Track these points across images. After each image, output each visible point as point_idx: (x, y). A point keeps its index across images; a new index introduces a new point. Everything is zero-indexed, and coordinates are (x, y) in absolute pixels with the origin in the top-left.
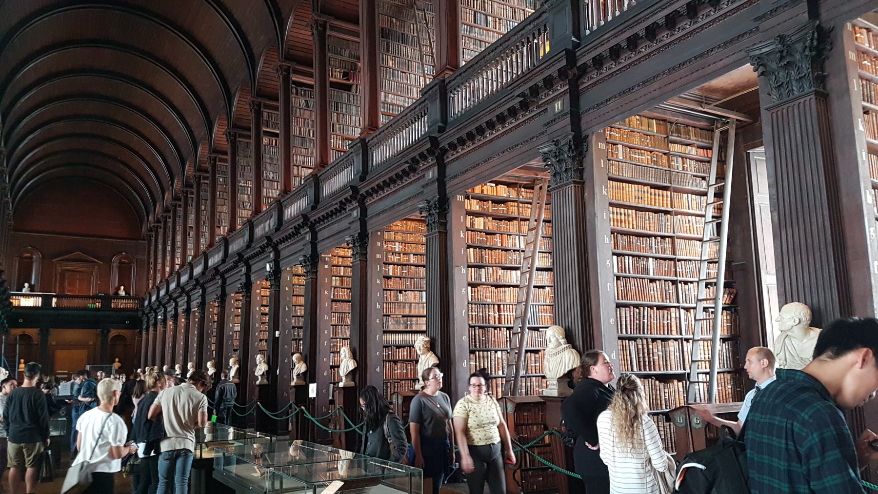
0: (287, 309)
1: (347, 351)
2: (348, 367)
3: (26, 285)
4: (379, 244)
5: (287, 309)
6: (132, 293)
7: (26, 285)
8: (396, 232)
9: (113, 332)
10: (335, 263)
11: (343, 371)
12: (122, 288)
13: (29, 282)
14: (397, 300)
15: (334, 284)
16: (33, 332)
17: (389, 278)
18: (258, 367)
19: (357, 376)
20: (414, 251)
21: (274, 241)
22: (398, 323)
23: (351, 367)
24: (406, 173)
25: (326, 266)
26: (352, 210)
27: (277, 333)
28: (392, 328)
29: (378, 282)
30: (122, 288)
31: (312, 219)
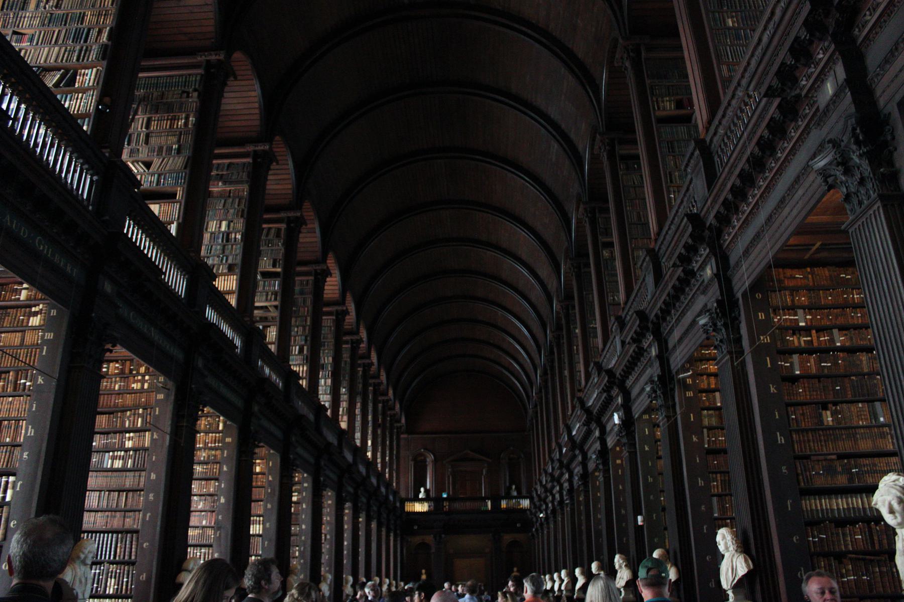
0: (650, 480)
1: (729, 537)
2: (734, 570)
3: (422, 490)
4: (761, 316)
5: (650, 480)
6: (524, 493)
7: (422, 490)
8: (794, 290)
9: (507, 538)
10: (704, 385)
11: (726, 581)
12: (514, 487)
14: (822, 422)
15: (706, 422)
16: (429, 539)
17: (794, 379)
18: (618, 575)
19: (758, 587)
20: (841, 321)
21: (618, 375)
22: (830, 471)
23: (742, 570)
24: (778, 129)
25: (690, 394)
26: (702, 267)
27: (640, 518)
28: (820, 482)
29: (772, 390)
30: (514, 487)
31: (652, 316)
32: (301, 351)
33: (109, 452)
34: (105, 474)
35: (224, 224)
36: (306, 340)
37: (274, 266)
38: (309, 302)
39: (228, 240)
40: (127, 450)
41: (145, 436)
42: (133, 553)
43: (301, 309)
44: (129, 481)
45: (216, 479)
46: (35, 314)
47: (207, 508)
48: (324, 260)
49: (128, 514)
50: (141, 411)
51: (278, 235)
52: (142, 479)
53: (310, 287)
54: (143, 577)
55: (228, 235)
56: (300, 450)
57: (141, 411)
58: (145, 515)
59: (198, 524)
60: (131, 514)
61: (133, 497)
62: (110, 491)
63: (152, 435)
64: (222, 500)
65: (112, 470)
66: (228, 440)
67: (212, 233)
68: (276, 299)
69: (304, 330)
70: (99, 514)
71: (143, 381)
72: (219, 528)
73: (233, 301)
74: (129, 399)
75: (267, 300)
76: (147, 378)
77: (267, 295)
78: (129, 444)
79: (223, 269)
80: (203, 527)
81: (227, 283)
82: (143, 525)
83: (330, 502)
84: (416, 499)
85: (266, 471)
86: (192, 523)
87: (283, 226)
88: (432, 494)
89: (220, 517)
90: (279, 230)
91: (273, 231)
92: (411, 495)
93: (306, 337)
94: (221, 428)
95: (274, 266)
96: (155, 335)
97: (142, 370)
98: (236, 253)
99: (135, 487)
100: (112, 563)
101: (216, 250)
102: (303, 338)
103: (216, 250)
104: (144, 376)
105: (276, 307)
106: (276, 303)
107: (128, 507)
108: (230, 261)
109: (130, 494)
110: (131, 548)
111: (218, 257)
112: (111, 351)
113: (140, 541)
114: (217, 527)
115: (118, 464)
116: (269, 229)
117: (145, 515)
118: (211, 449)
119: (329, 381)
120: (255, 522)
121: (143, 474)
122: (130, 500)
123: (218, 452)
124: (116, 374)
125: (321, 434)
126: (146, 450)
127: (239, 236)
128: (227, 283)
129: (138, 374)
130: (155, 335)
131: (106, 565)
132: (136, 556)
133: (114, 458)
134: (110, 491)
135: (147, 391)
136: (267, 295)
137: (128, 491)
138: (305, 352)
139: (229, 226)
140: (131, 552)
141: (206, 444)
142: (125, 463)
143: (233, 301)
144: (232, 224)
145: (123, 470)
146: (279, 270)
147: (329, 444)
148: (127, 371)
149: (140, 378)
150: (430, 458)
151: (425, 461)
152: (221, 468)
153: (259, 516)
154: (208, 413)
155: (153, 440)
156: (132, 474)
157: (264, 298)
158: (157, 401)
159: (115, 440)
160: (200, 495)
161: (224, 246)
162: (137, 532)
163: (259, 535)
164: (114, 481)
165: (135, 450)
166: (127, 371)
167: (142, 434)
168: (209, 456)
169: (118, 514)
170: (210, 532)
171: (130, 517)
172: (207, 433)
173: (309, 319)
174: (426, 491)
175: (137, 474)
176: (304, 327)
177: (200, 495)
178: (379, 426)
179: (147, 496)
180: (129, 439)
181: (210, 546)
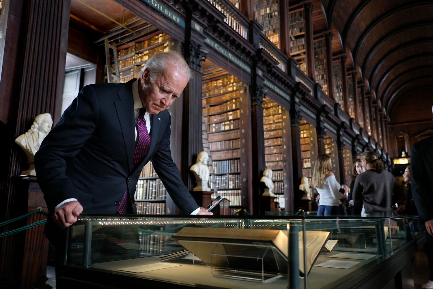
7: (403, 153)
13: (404, 151)
32: (323, 77)
33: (222, 123)
34: (222, 133)
35: (268, 9)
36: (325, 71)
37: (301, 31)
38: (324, 51)
39: (271, 17)
40: (230, 121)
41: (237, 112)
42: (239, 169)
43: (320, 56)
44: (233, 135)
45: (281, 137)
46: (165, 47)
47: (278, 152)
48: (330, 28)
49: (234, 151)
50: (234, 101)
51: (301, 15)
52: (239, 133)
53: (324, 42)
54: (244, 180)
55: (271, 14)
56: (326, 125)
57: (234, 101)
58: (242, 151)
59: (274, 160)
60: (236, 150)
61: (235, 142)
62: (225, 141)
63: (240, 111)
64: (285, 147)
65: (225, 131)
66: (285, 117)
67: (263, 16)
68: (304, 49)
69: (323, 66)
70: (222, 152)
71: (233, 86)
72: (285, 161)
73: (278, 47)
74: (227, 97)
75: (299, 50)
76: (235, 84)
77: (299, 48)
78: (231, 118)
79: (271, 32)
80: (277, 161)
81: (275, 39)
82: (241, 155)
83: (348, 155)
84: (400, 157)
85: (309, 136)
86: (265, 153)
87: (302, 9)
88: (409, 154)
89: (285, 156)
90: (301, 12)
91: (297, 13)
92: (397, 155)
93: (325, 70)
94: (280, 111)
95: (301, 31)
96: (230, 56)
97: (232, 81)
98: (276, 23)
99: (236, 137)
100: (230, 174)
101: (266, 23)
102: (323, 70)
103: (266, 23)
104: (233, 83)
105: (304, 53)
106: (304, 51)
107: (234, 148)
108: (274, 28)
109: (234, 141)
110: (237, 167)
111: (268, 27)
112: (204, 60)
113: (241, 163)
114: (284, 161)
115: (227, 128)
116: (295, 13)
117: (242, 151)
118: (277, 123)
119: (341, 94)
120: (306, 162)
121: (239, 130)
122: (234, 144)
123: (280, 124)
124: (221, 86)
125: (339, 118)
126: (238, 119)
127: (276, 13)
128: (275, 39)
129: (230, 83)
130: (230, 56)
131: (228, 175)
132: (240, 170)
133: (225, 125)
134: (225, 141)
135: (236, 91)
136: (299, 48)
137: (233, 140)
138: (325, 77)
139: (270, 10)
140: (237, 169)
141: (274, 121)
142: (230, 127)
143: (278, 47)
144: (272, 8)
145: (230, 130)
146: (303, 33)
147: (343, 122)
148: (225, 83)
149: (231, 85)
150: (406, 136)
151: (403, 138)
152: (283, 131)
153: (308, 158)
154: (273, 105)
155: (241, 114)
156: (233, 131)
157: (297, 49)
158: (240, 94)
159: (224, 116)
160: (274, 146)
161: (270, 20)
162: (239, 159)
163: (309, 168)
164: (227, 137)
165: (234, 120)
166: (225, 83)
167: (236, 111)
168: (276, 127)
169: (230, 151)
170: (281, 163)
171: (235, 152)
172: (273, 115)
173: (325, 60)
174: (406, 153)
175: (236, 131)
176: (323, 65)
177: (274, 146)
178: (374, 120)
179: (241, 141)
180: (231, 115)
181: (281, 170)
